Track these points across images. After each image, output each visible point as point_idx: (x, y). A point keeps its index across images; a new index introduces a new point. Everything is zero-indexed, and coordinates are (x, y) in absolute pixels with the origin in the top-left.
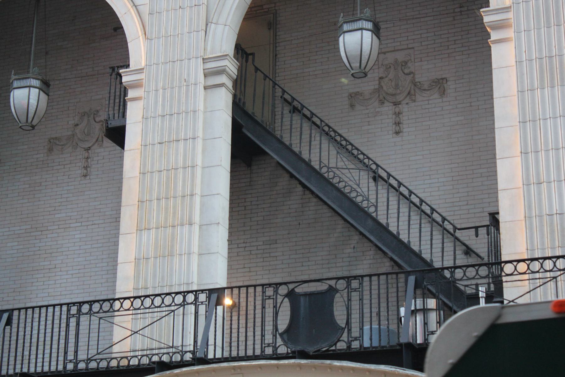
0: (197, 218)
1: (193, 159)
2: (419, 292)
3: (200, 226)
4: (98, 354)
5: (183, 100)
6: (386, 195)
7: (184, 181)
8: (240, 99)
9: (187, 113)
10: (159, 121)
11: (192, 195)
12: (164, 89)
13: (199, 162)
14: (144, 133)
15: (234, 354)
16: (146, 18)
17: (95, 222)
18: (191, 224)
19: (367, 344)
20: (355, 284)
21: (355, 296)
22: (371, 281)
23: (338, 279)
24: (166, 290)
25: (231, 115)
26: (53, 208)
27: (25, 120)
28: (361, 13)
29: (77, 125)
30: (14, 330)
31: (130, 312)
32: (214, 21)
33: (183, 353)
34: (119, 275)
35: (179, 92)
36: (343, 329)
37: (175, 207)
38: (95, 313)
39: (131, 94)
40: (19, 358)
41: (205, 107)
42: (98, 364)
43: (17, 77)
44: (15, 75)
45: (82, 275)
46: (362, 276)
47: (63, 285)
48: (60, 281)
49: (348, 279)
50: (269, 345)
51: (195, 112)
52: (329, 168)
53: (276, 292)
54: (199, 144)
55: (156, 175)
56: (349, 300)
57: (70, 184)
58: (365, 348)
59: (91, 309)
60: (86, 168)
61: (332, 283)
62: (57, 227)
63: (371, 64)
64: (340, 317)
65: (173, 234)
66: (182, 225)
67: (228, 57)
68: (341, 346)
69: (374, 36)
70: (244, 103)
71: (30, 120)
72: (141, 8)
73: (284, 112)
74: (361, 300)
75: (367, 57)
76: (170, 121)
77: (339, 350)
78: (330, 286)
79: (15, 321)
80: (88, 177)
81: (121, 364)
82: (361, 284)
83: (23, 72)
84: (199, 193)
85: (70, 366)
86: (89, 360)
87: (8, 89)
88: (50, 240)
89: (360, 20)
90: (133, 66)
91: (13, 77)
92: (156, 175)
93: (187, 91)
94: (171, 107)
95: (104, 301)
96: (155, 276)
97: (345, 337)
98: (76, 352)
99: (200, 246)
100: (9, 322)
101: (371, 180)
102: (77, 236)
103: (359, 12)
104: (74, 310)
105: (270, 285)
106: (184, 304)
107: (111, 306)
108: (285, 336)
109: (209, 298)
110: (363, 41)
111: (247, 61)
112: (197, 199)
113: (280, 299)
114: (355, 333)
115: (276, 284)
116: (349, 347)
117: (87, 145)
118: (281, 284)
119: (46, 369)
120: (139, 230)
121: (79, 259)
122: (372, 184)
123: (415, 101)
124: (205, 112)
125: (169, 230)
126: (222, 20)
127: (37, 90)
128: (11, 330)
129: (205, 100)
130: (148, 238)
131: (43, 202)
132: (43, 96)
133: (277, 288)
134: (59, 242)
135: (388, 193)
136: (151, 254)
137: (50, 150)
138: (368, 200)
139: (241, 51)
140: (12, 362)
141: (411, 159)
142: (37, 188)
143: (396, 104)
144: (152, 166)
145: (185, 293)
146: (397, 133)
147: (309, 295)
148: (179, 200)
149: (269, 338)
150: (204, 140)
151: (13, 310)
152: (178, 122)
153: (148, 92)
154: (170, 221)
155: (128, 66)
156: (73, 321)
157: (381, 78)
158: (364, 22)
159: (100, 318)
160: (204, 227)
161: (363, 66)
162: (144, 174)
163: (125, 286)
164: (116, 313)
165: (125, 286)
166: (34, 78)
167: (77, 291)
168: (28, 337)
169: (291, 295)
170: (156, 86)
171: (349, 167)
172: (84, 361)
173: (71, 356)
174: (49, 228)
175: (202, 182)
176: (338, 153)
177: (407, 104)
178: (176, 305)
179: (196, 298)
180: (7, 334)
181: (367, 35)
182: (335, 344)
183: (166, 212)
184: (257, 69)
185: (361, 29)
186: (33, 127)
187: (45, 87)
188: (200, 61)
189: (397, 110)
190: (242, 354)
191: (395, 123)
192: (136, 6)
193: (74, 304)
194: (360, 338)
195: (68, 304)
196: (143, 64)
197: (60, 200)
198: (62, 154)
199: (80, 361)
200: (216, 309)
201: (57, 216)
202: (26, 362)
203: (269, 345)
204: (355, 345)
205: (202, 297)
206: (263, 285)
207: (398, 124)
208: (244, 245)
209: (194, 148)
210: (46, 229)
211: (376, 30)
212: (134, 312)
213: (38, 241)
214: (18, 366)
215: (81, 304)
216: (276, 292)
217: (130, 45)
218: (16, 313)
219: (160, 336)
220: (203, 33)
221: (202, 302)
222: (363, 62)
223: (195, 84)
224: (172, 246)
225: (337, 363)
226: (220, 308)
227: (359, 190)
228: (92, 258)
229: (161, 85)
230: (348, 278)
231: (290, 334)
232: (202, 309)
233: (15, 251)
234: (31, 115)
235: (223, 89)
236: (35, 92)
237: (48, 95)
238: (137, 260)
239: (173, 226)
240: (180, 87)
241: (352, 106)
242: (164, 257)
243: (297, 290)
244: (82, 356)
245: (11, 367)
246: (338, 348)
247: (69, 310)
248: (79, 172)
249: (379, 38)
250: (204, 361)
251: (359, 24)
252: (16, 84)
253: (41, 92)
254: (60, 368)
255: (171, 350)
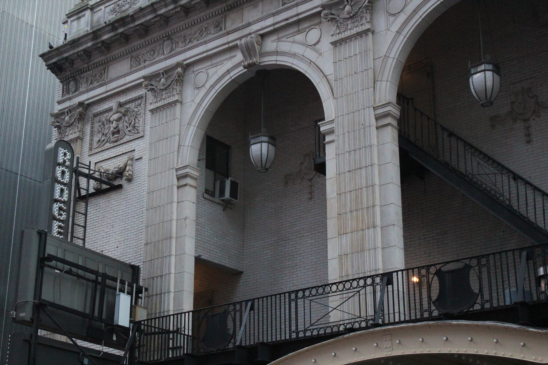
0: (378, 222)
1: (372, 180)
2: (531, 262)
3: (382, 228)
4: (311, 325)
5: (362, 139)
6: (524, 190)
7: (367, 197)
8: (404, 133)
9: (365, 147)
10: (347, 155)
11: (373, 206)
12: (349, 132)
13: (377, 181)
14: (338, 166)
15: (413, 318)
16: (333, 83)
17: (320, 231)
18: (374, 227)
19: (495, 305)
20: (484, 261)
21: (484, 270)
22: (494, 257)
23: (471, 258)
24: (361, 276)
25: (398, 145)
26: (291, 224)
27: (260, 165)
28: (484, 59)
29: (302, 163)
30: (256, 311)
31: (344, 292)
32: (379, 79)
33: (367, 321)
34: (330, 268)
35: (359, 133)
36: (478, 295)
37: (362, 216)
38: (307, 297)
39: (328, 139)
40: (278, 330)
41: (378, 142)
42: (312, 332)
43: (252, 136)
44: (251, 135)
45: (314, 269)
46: (488, 255)
47: (302, 277)
48: (300, 275)
49: (478, 258)
50: (426, 311)
51: (371, 146)
52: (473, 175)
53: (428, 272)
54: (376, 168)
55: (348, 195)
56: (480, 272)
57: (301, 205)
58: (494, 308)
59: (304, 295)
60: (311, 193)
61: (467, 262)
62: (295, 237)
63: (494, 95)
64: (475, 287)
65: (363, 235)
66: (368, 228)
67: (390, 104)
68: (477, 307)
69: (495, 75)
70: (409, 135)
71: (264, 165)
72: (329, 77)
73: (444, 137)
74: (489, 272)
75: (491, 90)
76: (355, 154)
77: (475, 310)
78: (466, 264)
79: (256, 306)
80: (313, 200)
81: (320, 333)
82: (488, 261)
83: (256, 132)
84: (378, 204)
85: (294, 336)
86: (305, 331)
87: (247, 146)
88: (291, 246)
89: (482, 64)
90: (327, 120)
91: (250, 137)
92: (348, 195)
93: (364, 131)
94: (354, 145)
95: (312, 288)
96: (353, 267)
97: (479, 300)
98: (297, 326)
99: (382, 242)
100: (252, 308)
101: (511, 180)
102: (309, 242)
103: (482, 58)
104: (293, 296)
105: (423, 267)
106: (365, 286)
107: (317, 290)
108: (437, 303)
109: (382, 280)
110: (487, 79)
111: (408, 104)
112: (378, 209)
113: (431, 276)
114: (486, 297)
115: (427, 266)
116: (483, 307)
117: (310, 177)
118: (431, 266)
119: (278, 339)
120: (340, 235)
121: (312, 258)
122: (512, 182)
123: (539, 117)
124: (378, 145)
125: (360, 233)
126: (385, 78)
127: (267, 144)
128: (254, 313)
129: (378, 137)
130: (346, 240)
131: (284, 220)
132: (271, 147)
133: (429, 269)
134: (297, 247)
135: (526, 188)
136: (349, 251)
137: (286, 183)
138: (503, 196)
139: (402, 97)
140: (274, 334)
141: (540, 160)
142: (279, 211)
143: (525, 120)
144: (345, 189)
145: (365, 278)
146: (528, 142)
147: (452, 272)
148: (365, 211)
149: (425, 306)
150: (379, 165)
151: (254, 299)
152: (360, 155)
153: (338, 136)
154: (360, 227)
155: (323, 119)
156: (293, 304)
157: (513, 103)
158: (486, 65)
159: (310, 300)
160: (384, 228)
161: (488, 97)
162: (340, 194)
163: (333, 276)
164: (330, 295)
165: (333, 276)
166: (264, 136)
167: (312, 281)
168: (283, 315)
169: (439, 273)
170: (344, 131)
171: (487, 173)
172: (302, 331)
173: (293, 328)
174: (290, 238)
175: (380, 196)
176: (478, 163)
177: (534, 119)
178: (360, 287)
179: (373, 281)
180: (252, 315)
181: (489, 74)
182: (473, 306)
183: (357, 220)
184: (415, 109)
185: (484, 71)
186: (267, 170)
187: (273, 141)
188: (372, 109)
189: (527, 125)
190: (392, 321)
191: (526, 135)
192: (326, 76)
193: (293, 292)
194: (491, 301)
195: (289, 292)
196: (334, 117)
197: (295, 218)
198: (294, 185)
199: (300, 331)
200: (387, 288)
201: (294, 229)
202: (283, 333)
203: (426, 311)
204: (487, 306)
205: (378, 280)
206: (418, 268)
207: (528, 135)
208: (423, 237)
209: (372, 172)
210: (288, 239)
211: (497, 70)
212: (341, 293)
213: (283, 248)
214: (278, 336)
215: (297, 292)
216: (428, 272)
217: (324, 104)
218: (256, 300)
219: (349, 310)
220: (372, 89)
221: (377, 284)
222: (488, 95)
223: (370, 126)
224: (363, 244)
225: (454, 322)
226: (390, 287)
227: (496, 190)
228: (319, 256)
229: (346, 130)
230: (478, 257)
231: (440, 302)
232: (378, 288)
233: (269, 256)
234: (264, 162)
235: (389, 128)
236: (265, 145)
237: (274, 145)
238: (340, 257)
239: (363, 230)
240: (359, 130)
241: (493, 126)
242: (358, 252)
243: (443, 269)
244: (301, 327)
245: (274, 337)
246: (475, 308)
247: (290, 296)
248: (306, 196)
249: (499, 74)
250: (378, 325)
251: (482, 67)
252: (252, 141)
253: (270, 145)
254: (288, 338)
255: (358, 320)
